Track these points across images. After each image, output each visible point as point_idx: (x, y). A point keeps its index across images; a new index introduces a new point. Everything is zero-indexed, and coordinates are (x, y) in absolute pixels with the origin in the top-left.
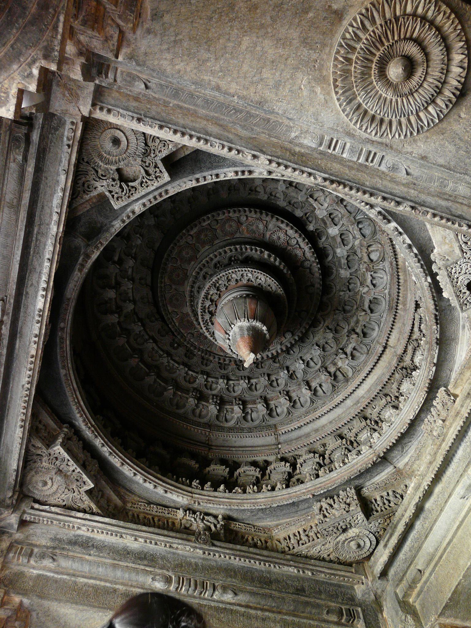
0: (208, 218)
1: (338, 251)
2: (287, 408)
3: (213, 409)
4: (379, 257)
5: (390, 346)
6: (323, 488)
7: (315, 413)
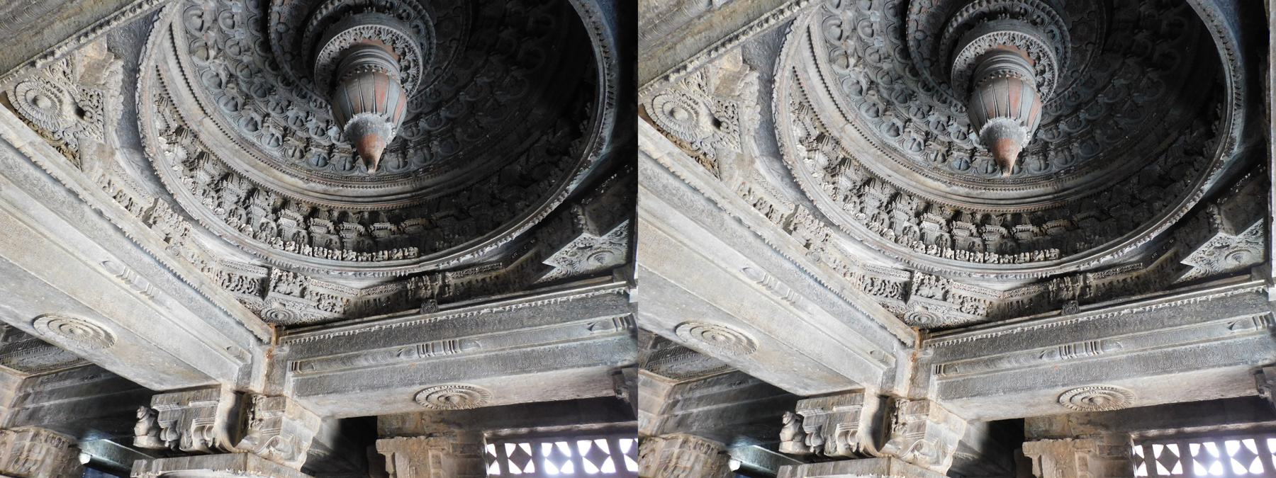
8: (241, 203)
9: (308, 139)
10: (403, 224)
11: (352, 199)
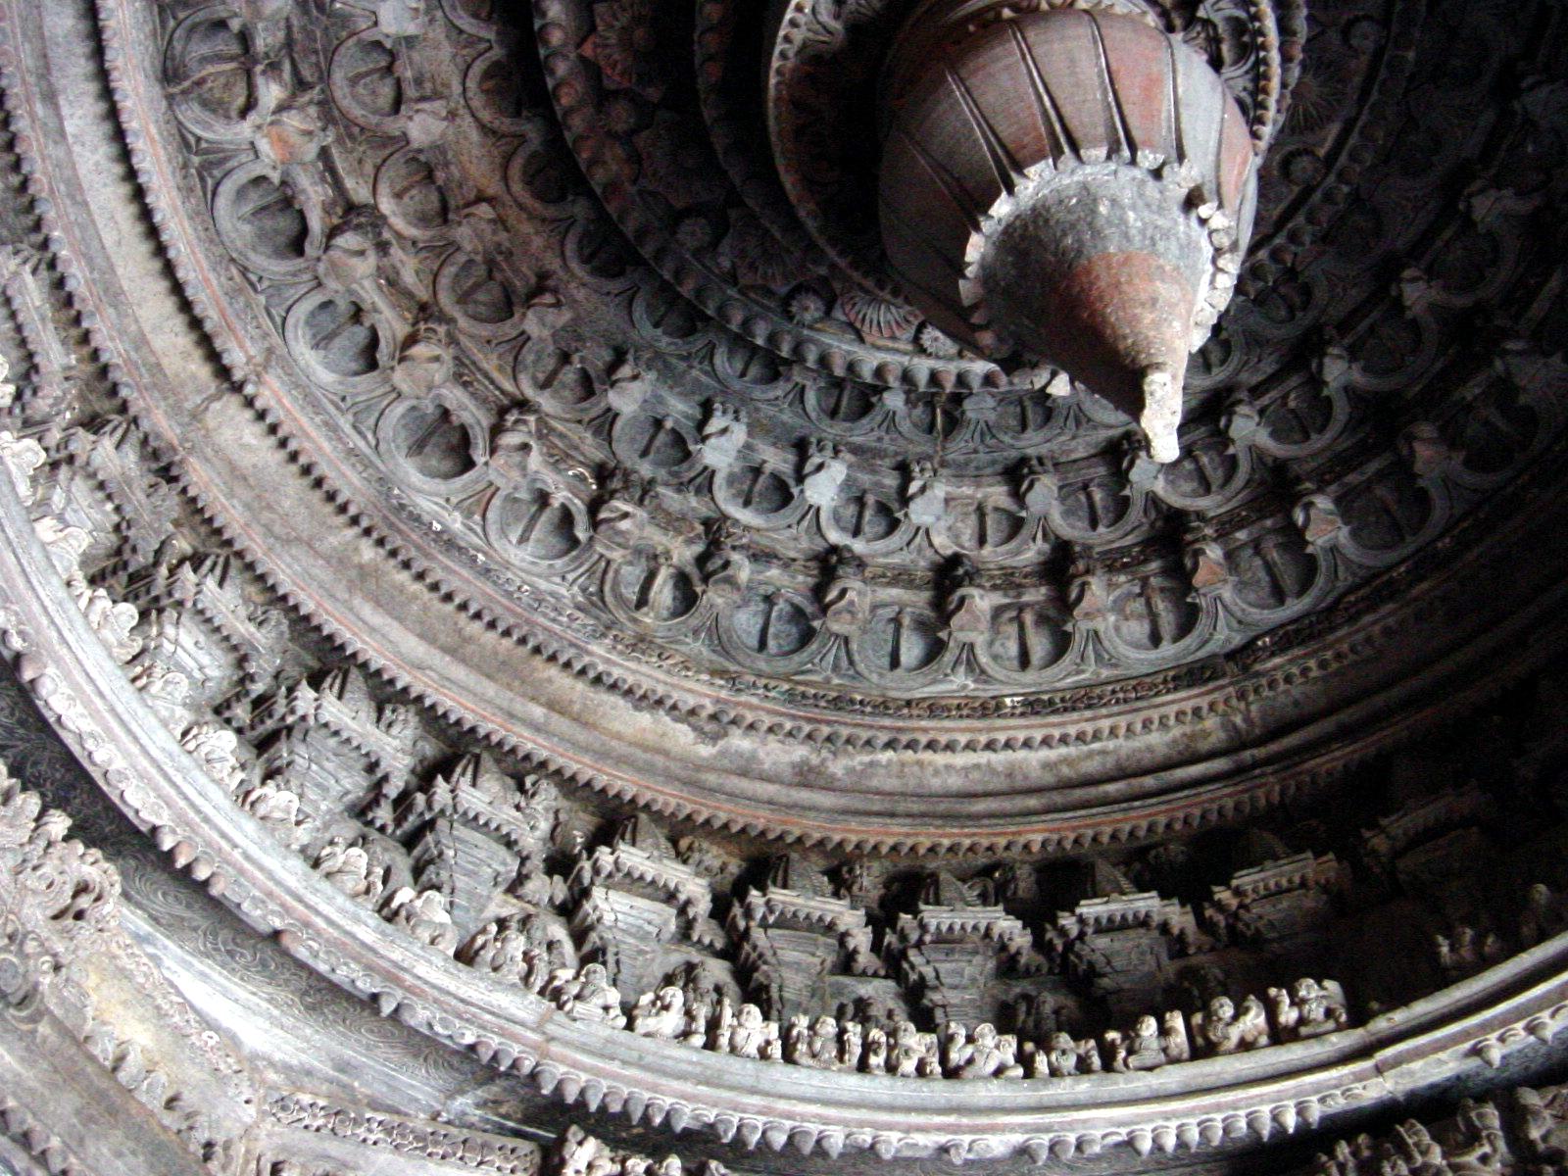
5: (217, 397)
8: (384, 814)
9: (715, 531)
10: (1222, 894)
11: (943, 806)
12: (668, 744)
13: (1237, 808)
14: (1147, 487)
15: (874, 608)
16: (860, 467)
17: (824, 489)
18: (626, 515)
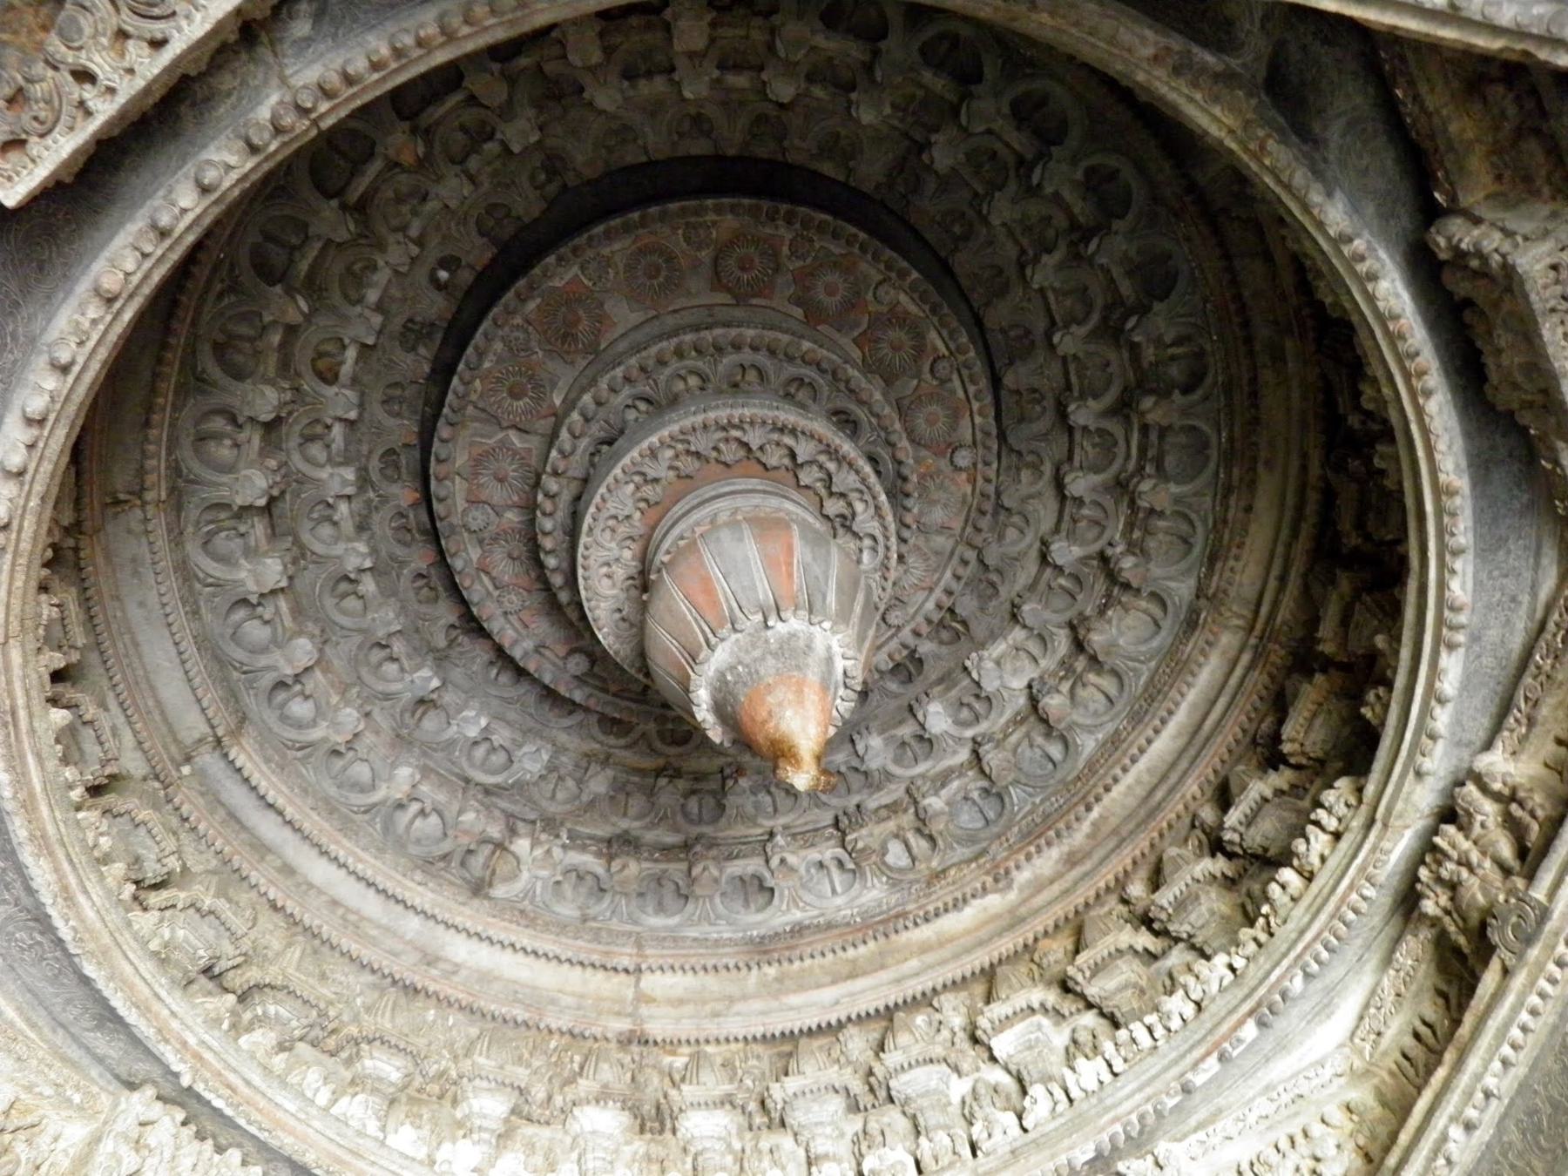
0: (961, 350)
1: (876, 741)
2: (325, 740)
3: (253, 485)
4: (901, 870)
5: (638, 981)
6: (236, 1100)
7: (339, 836)
12: (992, 911)
13: (1270, 675)
14: (1070, 558)
15: (1015, 751)
16: (948, 689)
17: (937, 717)
18: (856, 841)
